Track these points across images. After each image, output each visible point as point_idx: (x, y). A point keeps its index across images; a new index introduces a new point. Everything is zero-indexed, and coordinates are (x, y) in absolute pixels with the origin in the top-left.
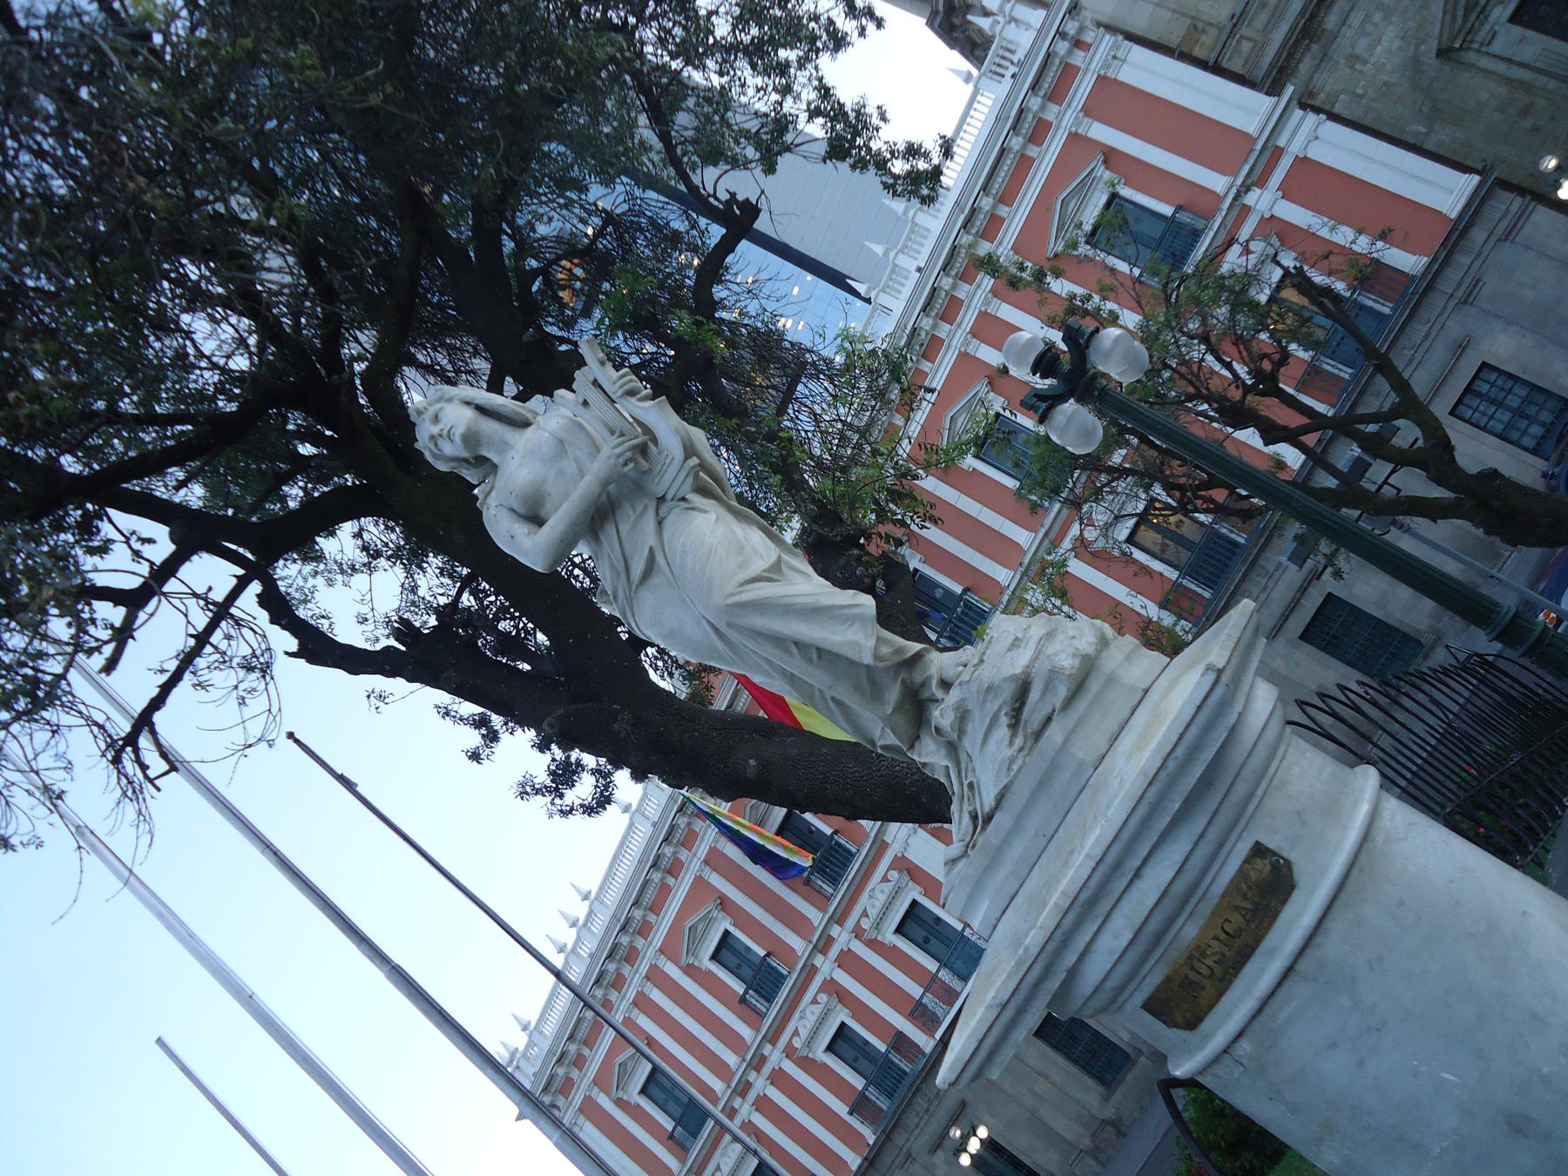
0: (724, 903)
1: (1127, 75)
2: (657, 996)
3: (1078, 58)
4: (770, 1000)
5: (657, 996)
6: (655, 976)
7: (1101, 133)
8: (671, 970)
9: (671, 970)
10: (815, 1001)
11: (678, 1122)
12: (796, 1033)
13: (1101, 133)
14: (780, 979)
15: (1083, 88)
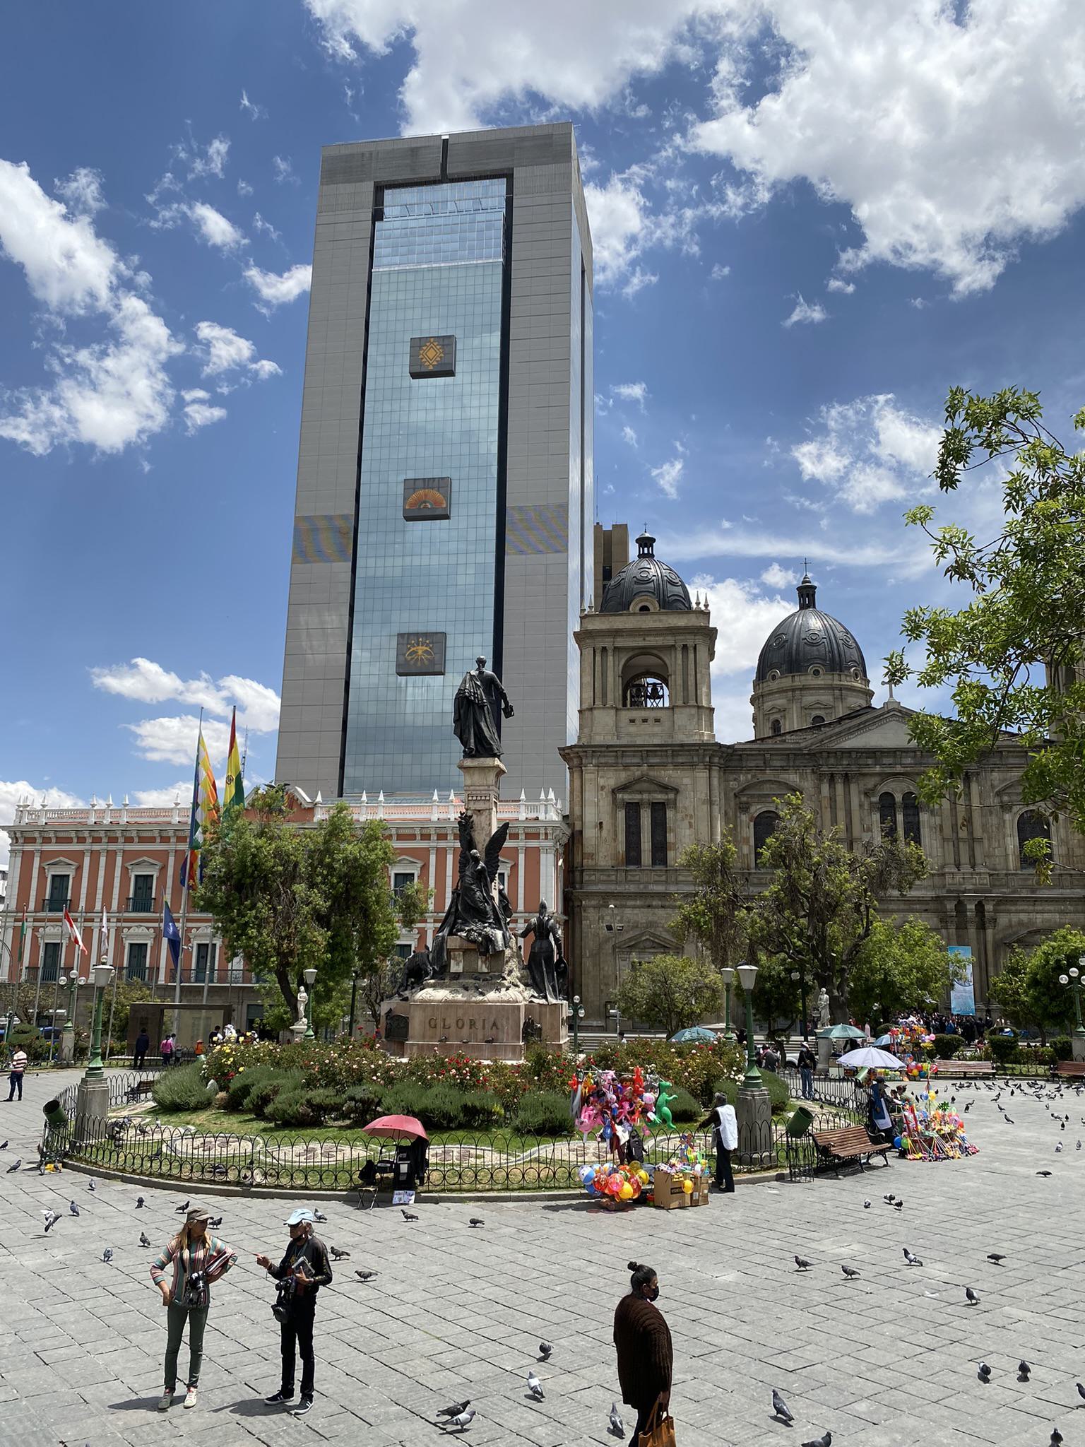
0: (164, 869)
1: (543, 856)
2: (103, 860)
3: (542, 837)
4: (134, 910)
5: (103, 860)
6: (111, 855)
7: (522, 857)
8: (119, 860)
9: (119, 860)
10: (148, 928)
11: (50, 900)
12: (129, 928)
13: (522, 857)
14: (146, 909)
15: (533, 844)
